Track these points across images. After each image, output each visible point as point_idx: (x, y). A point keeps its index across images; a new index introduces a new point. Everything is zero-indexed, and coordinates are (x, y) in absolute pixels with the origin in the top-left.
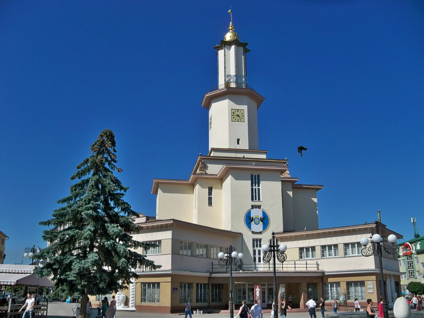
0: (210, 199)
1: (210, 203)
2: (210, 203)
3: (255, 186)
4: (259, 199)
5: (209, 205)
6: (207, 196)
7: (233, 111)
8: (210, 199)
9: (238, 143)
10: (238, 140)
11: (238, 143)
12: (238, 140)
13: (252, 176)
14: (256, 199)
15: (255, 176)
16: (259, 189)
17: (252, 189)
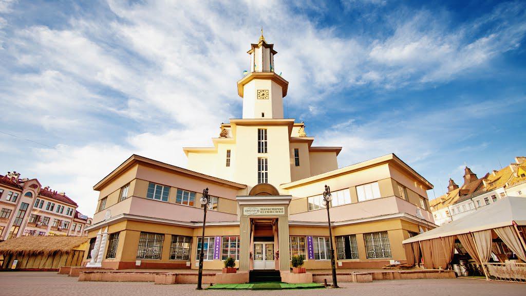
0: (228, 161)
1: (228, 165)
2: (228, 165)
3: (263, 139)
4: (266, 152)
5: (227, 166)
6: (225, 158)
7: (259, 91)
8: (228, 161)
9: (263, 116)
10: (263, 115)
11: (263, 116)
12: (263, 115)
13: (259, 130)
14: (263, 152)
15: (262, 130)
16: (266, 143)
17: (259, 143)
